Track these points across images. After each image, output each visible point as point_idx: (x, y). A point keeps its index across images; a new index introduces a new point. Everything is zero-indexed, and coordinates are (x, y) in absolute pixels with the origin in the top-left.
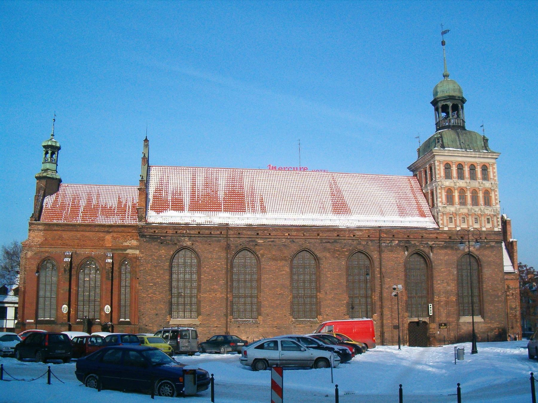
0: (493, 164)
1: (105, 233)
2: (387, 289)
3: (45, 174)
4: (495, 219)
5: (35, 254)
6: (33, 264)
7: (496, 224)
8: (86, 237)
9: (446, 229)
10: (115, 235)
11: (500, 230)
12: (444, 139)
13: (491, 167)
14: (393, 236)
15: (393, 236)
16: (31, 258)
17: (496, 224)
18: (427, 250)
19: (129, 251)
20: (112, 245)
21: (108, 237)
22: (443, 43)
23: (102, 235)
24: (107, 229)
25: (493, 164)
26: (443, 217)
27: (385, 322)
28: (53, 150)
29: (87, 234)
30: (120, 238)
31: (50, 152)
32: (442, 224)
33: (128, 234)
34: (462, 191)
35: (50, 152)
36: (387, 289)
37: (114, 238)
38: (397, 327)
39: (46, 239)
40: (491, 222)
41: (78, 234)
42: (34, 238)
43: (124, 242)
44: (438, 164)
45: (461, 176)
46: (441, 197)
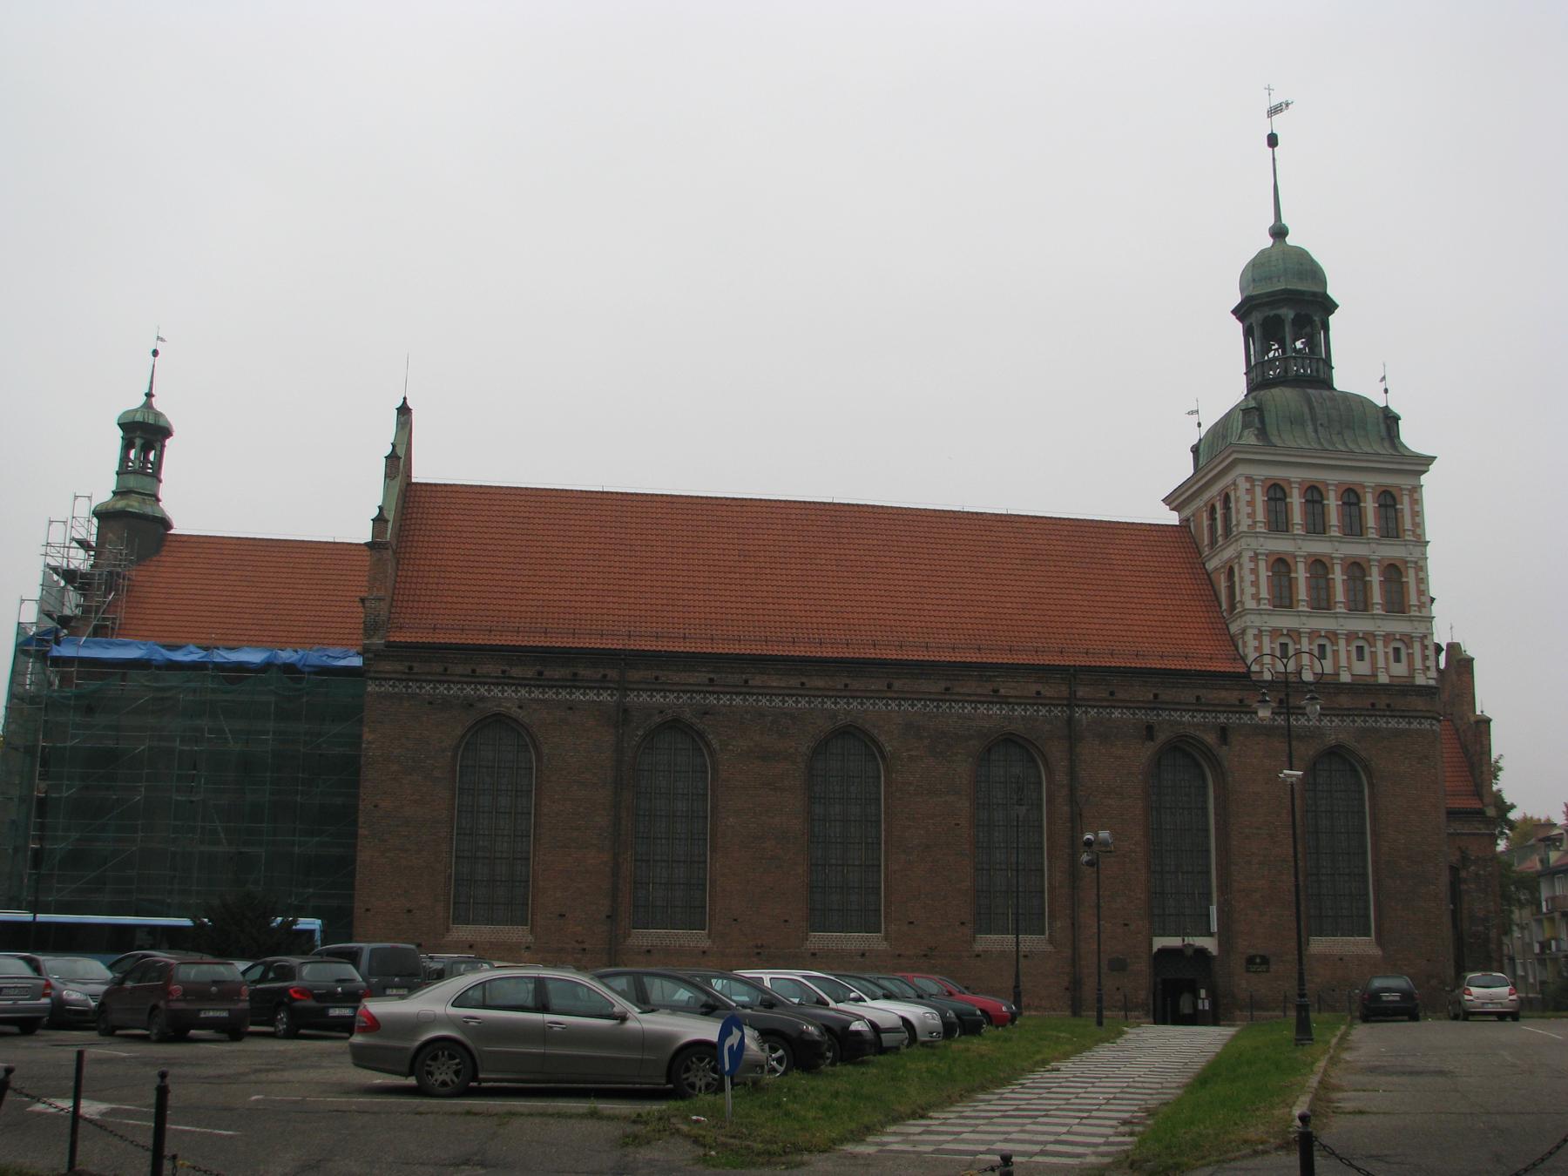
3: (121, 504)
4: (1417, 646)
7: (1418, 664)
11: (1432, 682)
12: (1266, 414)
13: (1406, 499)
14: (1112, 694)
15: (1112, 694)
18: (1210, 739)
22: (1273, 141)
26: (1261, 642)
31: (138, 442)
35: (138, 442)
44: (1248, 486)
45: (1316, 526)
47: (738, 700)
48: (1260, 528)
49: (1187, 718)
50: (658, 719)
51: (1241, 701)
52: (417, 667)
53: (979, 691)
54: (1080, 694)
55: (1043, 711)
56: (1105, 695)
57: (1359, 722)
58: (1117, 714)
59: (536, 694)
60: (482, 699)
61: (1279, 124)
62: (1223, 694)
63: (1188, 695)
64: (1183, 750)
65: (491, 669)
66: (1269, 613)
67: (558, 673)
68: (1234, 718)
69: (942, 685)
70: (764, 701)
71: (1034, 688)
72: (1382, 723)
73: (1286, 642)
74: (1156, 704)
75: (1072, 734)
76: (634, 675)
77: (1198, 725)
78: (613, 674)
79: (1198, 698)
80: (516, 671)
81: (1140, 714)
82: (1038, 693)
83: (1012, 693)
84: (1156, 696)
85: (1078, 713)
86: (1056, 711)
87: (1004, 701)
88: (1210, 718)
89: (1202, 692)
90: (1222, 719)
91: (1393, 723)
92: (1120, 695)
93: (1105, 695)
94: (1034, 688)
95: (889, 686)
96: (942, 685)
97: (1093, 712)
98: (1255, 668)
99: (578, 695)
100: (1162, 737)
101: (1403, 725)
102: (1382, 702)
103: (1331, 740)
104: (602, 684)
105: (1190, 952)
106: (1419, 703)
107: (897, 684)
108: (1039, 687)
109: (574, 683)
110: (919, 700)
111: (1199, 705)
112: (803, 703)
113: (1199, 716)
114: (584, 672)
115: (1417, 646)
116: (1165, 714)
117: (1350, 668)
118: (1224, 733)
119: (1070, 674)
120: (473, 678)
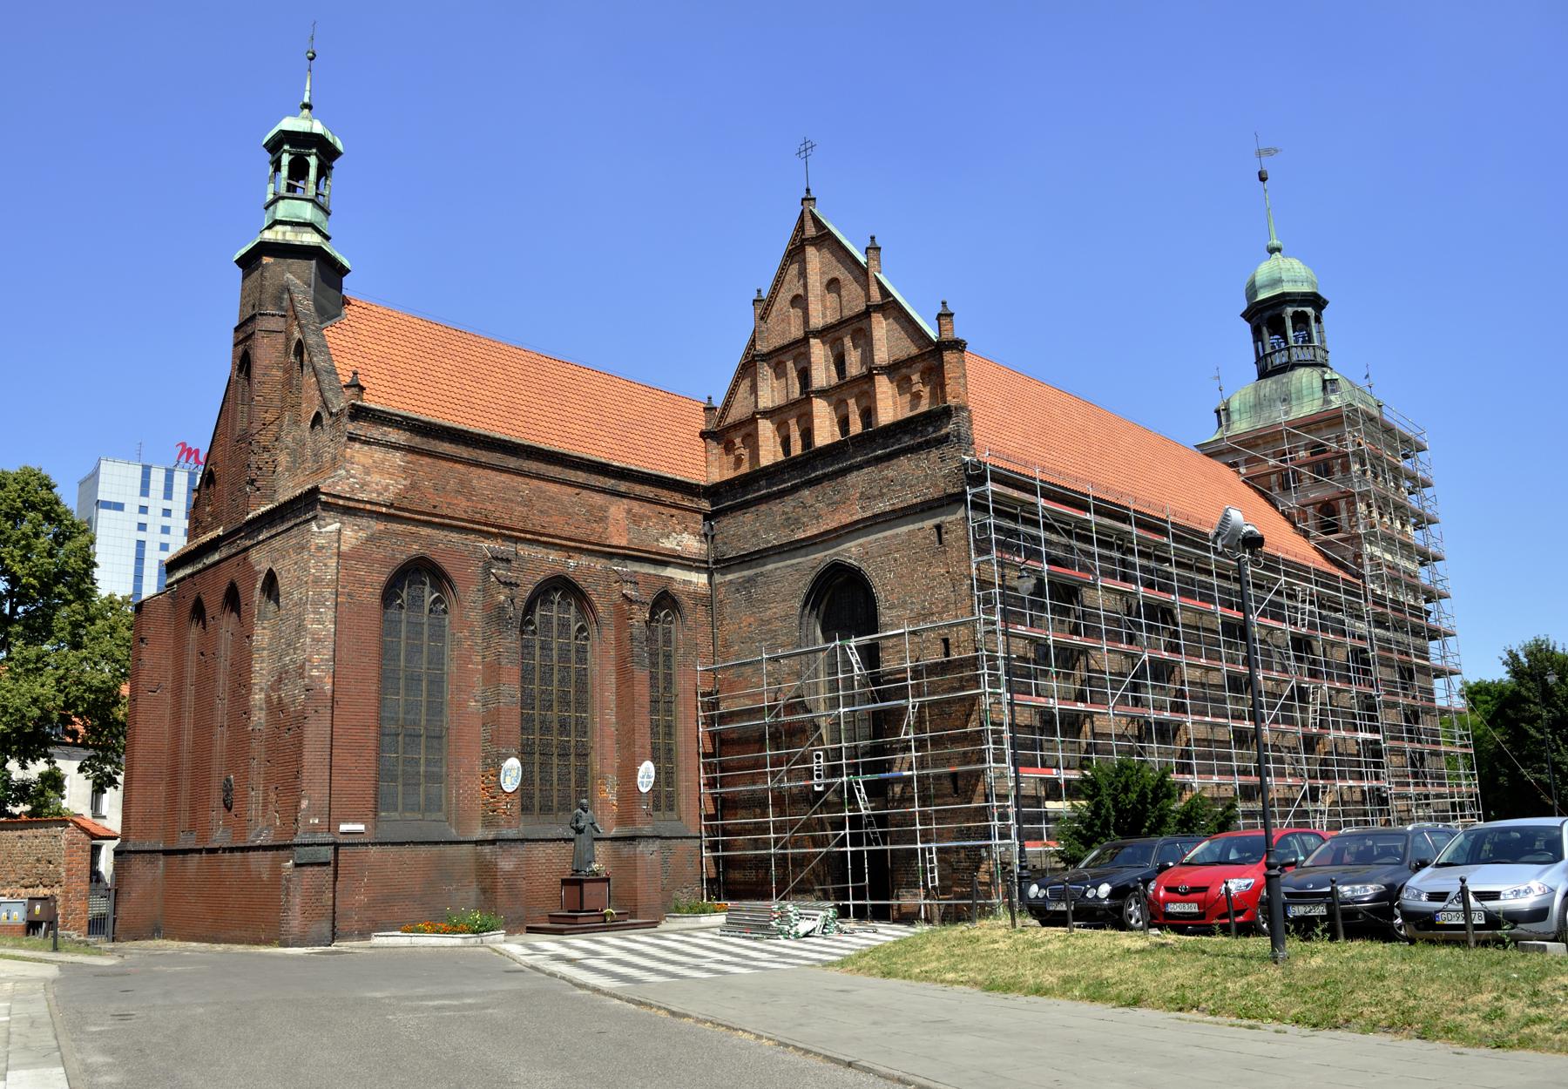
1: (608, 497)
5: (370, 539)
6: (362, 582)
8: (551, 499)
10: (636, 507)
16: (356, 555)
19: (670, 572)
20: (630, 541)
21: (618, 510)
22: (1263, 179)
23: (599, 499)
24: (610, 483)
28: (305, 156)
29: (553, 488)
30: (649, 518)
33: (674, 511)
37: (636, 519)
39: (413, 486)
41: (526, 486)
42: (367, 471)
43: (662, 535)
61: (1268, 165)
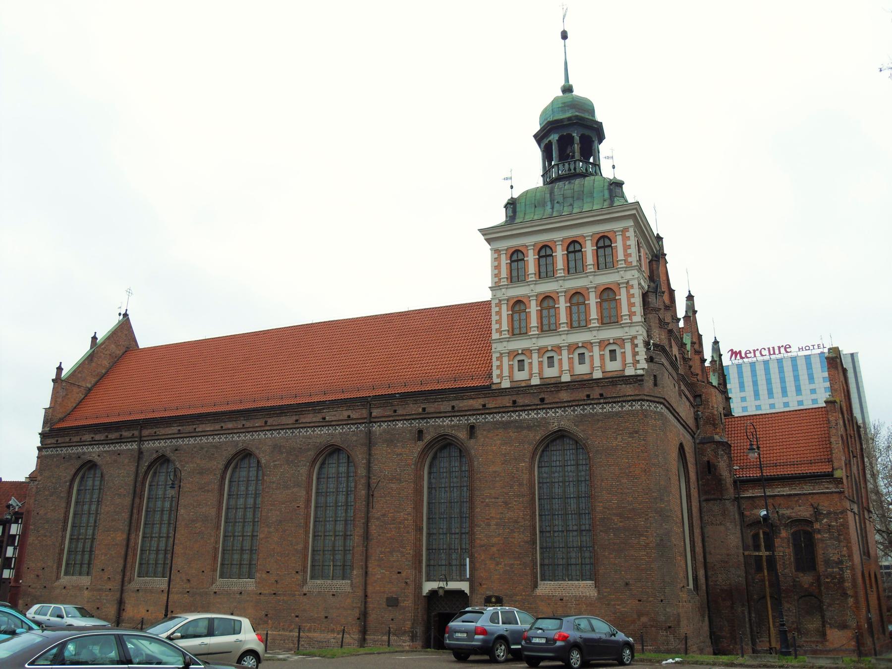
0: (626, 230)
2: (378, 519)
4: (628, 346)
7: (629, 359)
9: (506, 384)
11: (640, 372)
15: (395, 411)
17: (629, 359)
18: (462, 435)
25: (626, 230)
27: (370, 589)
32: (498, 376)
34: (577, 297)
36: (378, 519)
38: (393, 602)
40: (587, 360)
46: (499, 322)
47: (192, 441)
48: (504, 282)
49: (447, 422)
50: (155, 456)
51: (484, 406)
52: (60, 440)
53: (314, 419)
54: (374, 414)
55: (353, 428)
56: (391, 413)
57: (579, 410)
58: (400, 424)
59: (107, 448)
60: (84, 453)
62: (471, 402)
63: (445, 406)
64: (444, 444)
65: (87, 437)
66: (508, 340)
67: (113, 436)
68: (481, 419)
69: (295, 418)
70: (204, 440)
71: (345, 414)
72: (598, 409)
73: (520, 359)
74: (425, 415)
75: (370, 442)
76: (145, 432)
77: (454, 426)
78: (136, 433)
79: (453, 407)
80: (97, 437)
81: (415, 424)
82: (349, 416)
83: (334, 418)
84: (424, 409)
85: (375, 428)
86: (362, 427)
87: (329, 424)
88: (464, 421)
89: (454, 403)
90: (472, 420)
91: (608, 408)
92: (400, 412)
93: (391, 413)
94: (345, 414)
95: (266, 422)
96: (295, 418)
97: (384, 425)
98: (496, 380)
99: (124, 447)
100: (428, 438)
101: (617, 408)
102: (595, 393)
103: (555, 427)
104: (131, 439)
105: (441, 593)
106: (628, 390)
107: (270, 421)
108: (349, 413)
109: (121, 440)
110: (282, 429)
111: (454, 412)
112: (223, 439)
113: (455, 420)
114: (126, 434)
115: (628, 346)
116: (432, 422)
117: (564, 369)
118: (472, 429)
119: (365, 402)
120: (81, 443)
